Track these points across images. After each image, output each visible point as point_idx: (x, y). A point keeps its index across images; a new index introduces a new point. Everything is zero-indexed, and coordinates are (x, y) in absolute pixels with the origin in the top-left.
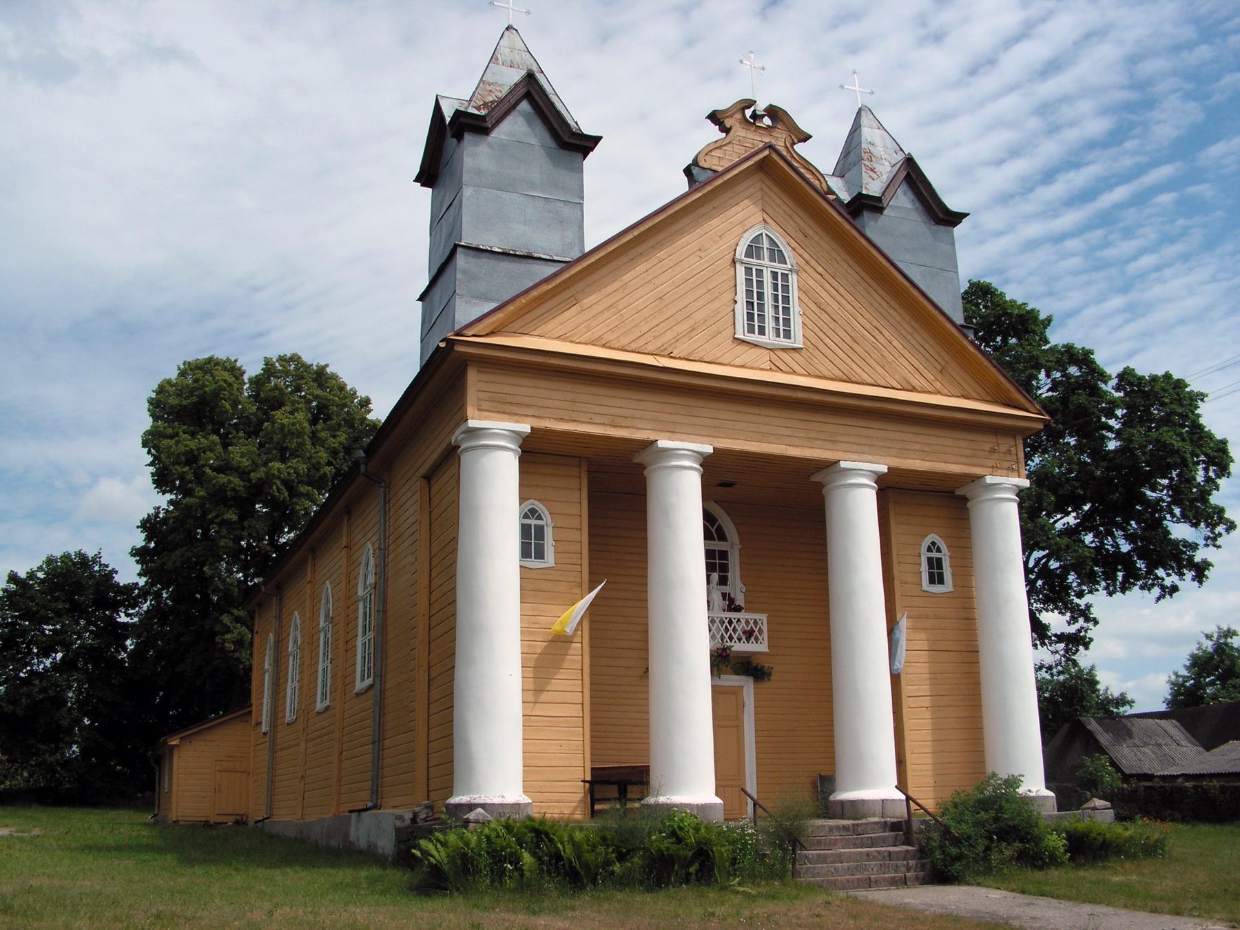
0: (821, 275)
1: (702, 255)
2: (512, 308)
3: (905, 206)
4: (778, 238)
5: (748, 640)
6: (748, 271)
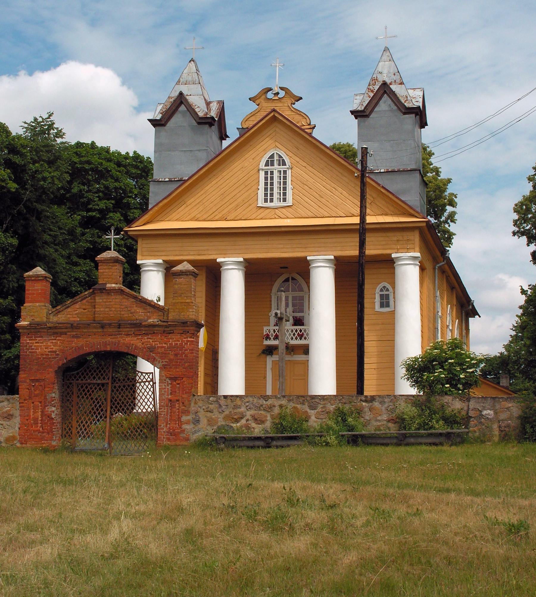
0: (305, 167)
1: (243, 169)
2: (152, 212)
3: (384, 109)
4: (282, 153)
5: (301, 339)
6: (266, 173)
